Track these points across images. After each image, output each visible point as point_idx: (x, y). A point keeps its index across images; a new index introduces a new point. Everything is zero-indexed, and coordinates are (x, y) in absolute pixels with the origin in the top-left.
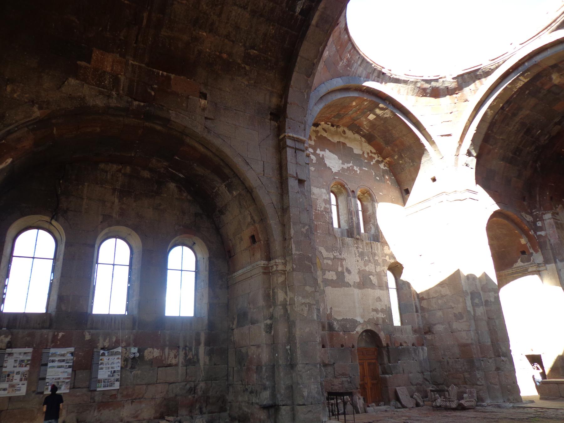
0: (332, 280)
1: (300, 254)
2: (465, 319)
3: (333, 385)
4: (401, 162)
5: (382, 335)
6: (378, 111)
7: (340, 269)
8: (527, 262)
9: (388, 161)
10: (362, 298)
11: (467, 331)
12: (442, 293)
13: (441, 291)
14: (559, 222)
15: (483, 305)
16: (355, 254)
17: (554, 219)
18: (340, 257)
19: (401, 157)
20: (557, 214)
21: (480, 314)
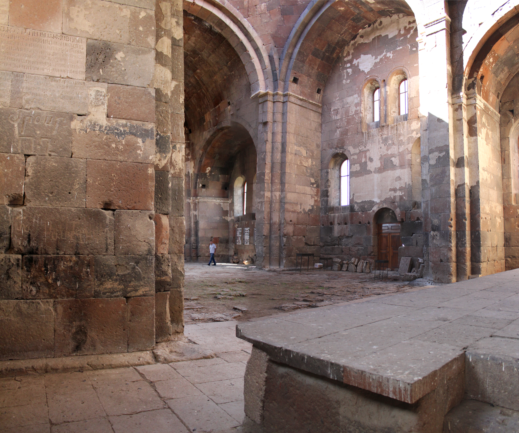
0: (356, 171)
3: (352, 251)
5: (398, 211)
7: (363, 160)
10: (381, 181)
16: (379, 142)
18: (365, 149)
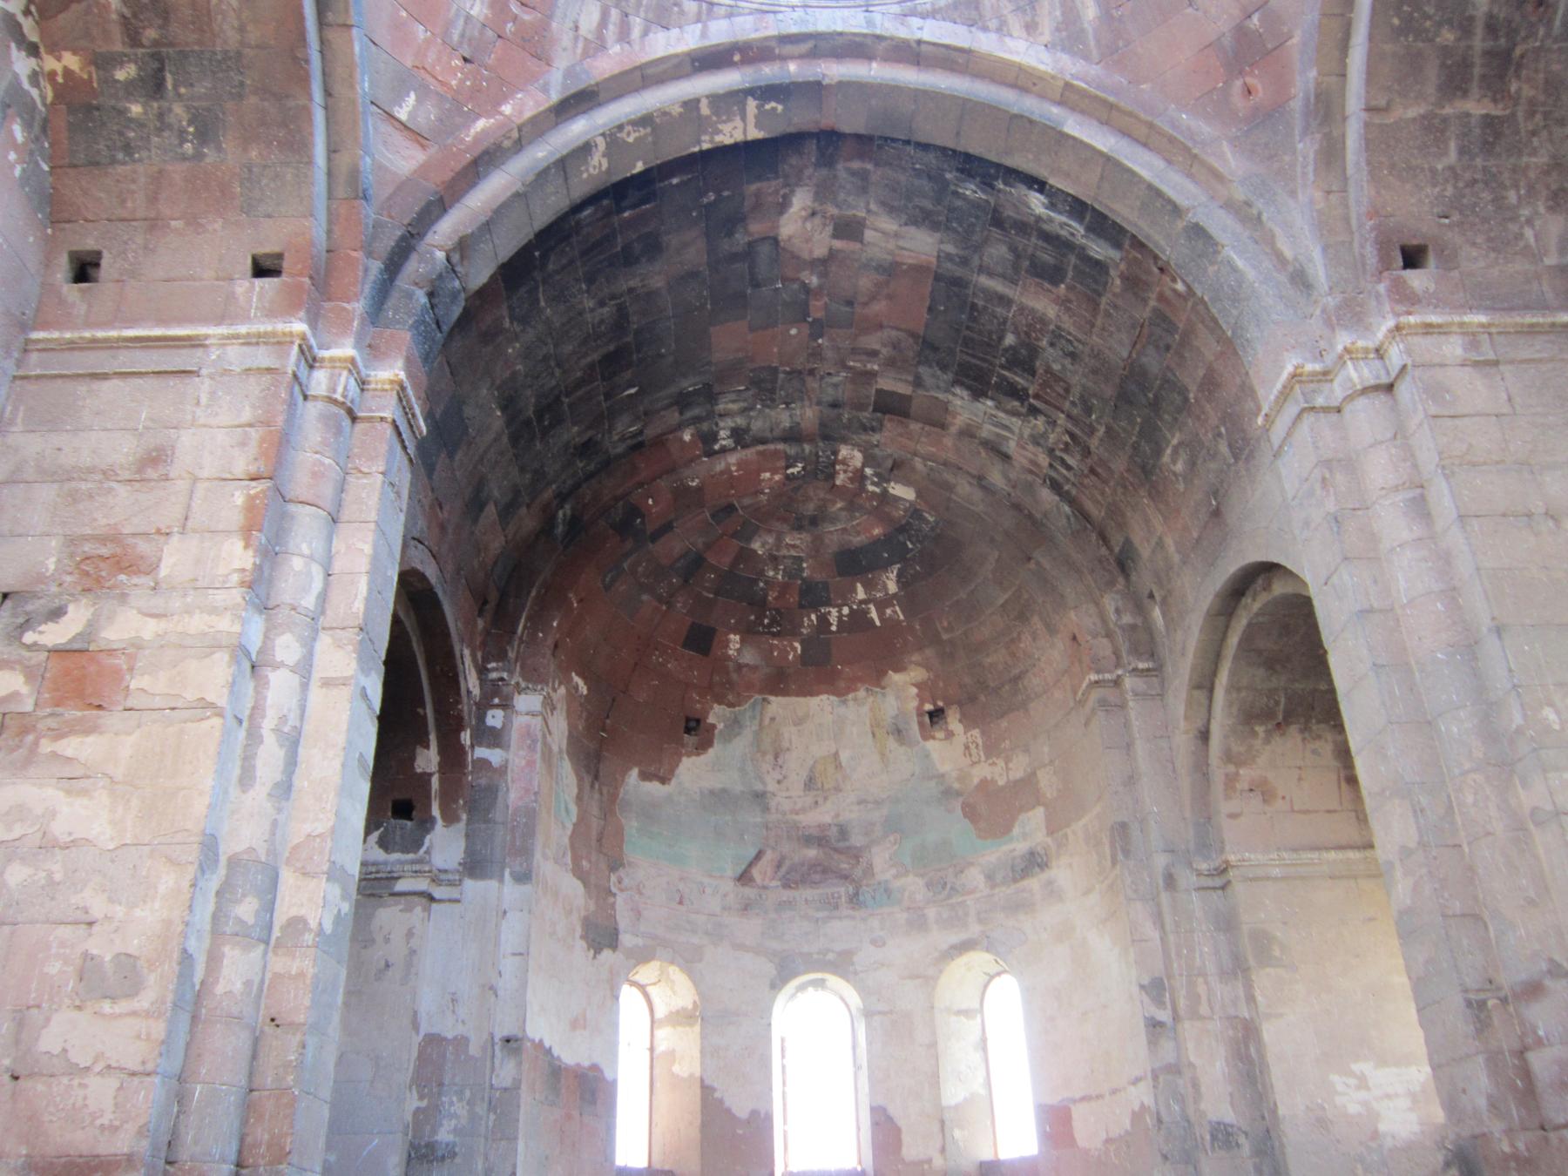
2: (144, 1002)
4: (136, 109)
8: (403, 852)
9: (67, 72)
11: (133, 1074)
12: (59, 829)
13: (52, 814)
14: (549, 739)
15: (267, 943)
19: (153, 85)
20: (553, 708)
21: (238, 986)
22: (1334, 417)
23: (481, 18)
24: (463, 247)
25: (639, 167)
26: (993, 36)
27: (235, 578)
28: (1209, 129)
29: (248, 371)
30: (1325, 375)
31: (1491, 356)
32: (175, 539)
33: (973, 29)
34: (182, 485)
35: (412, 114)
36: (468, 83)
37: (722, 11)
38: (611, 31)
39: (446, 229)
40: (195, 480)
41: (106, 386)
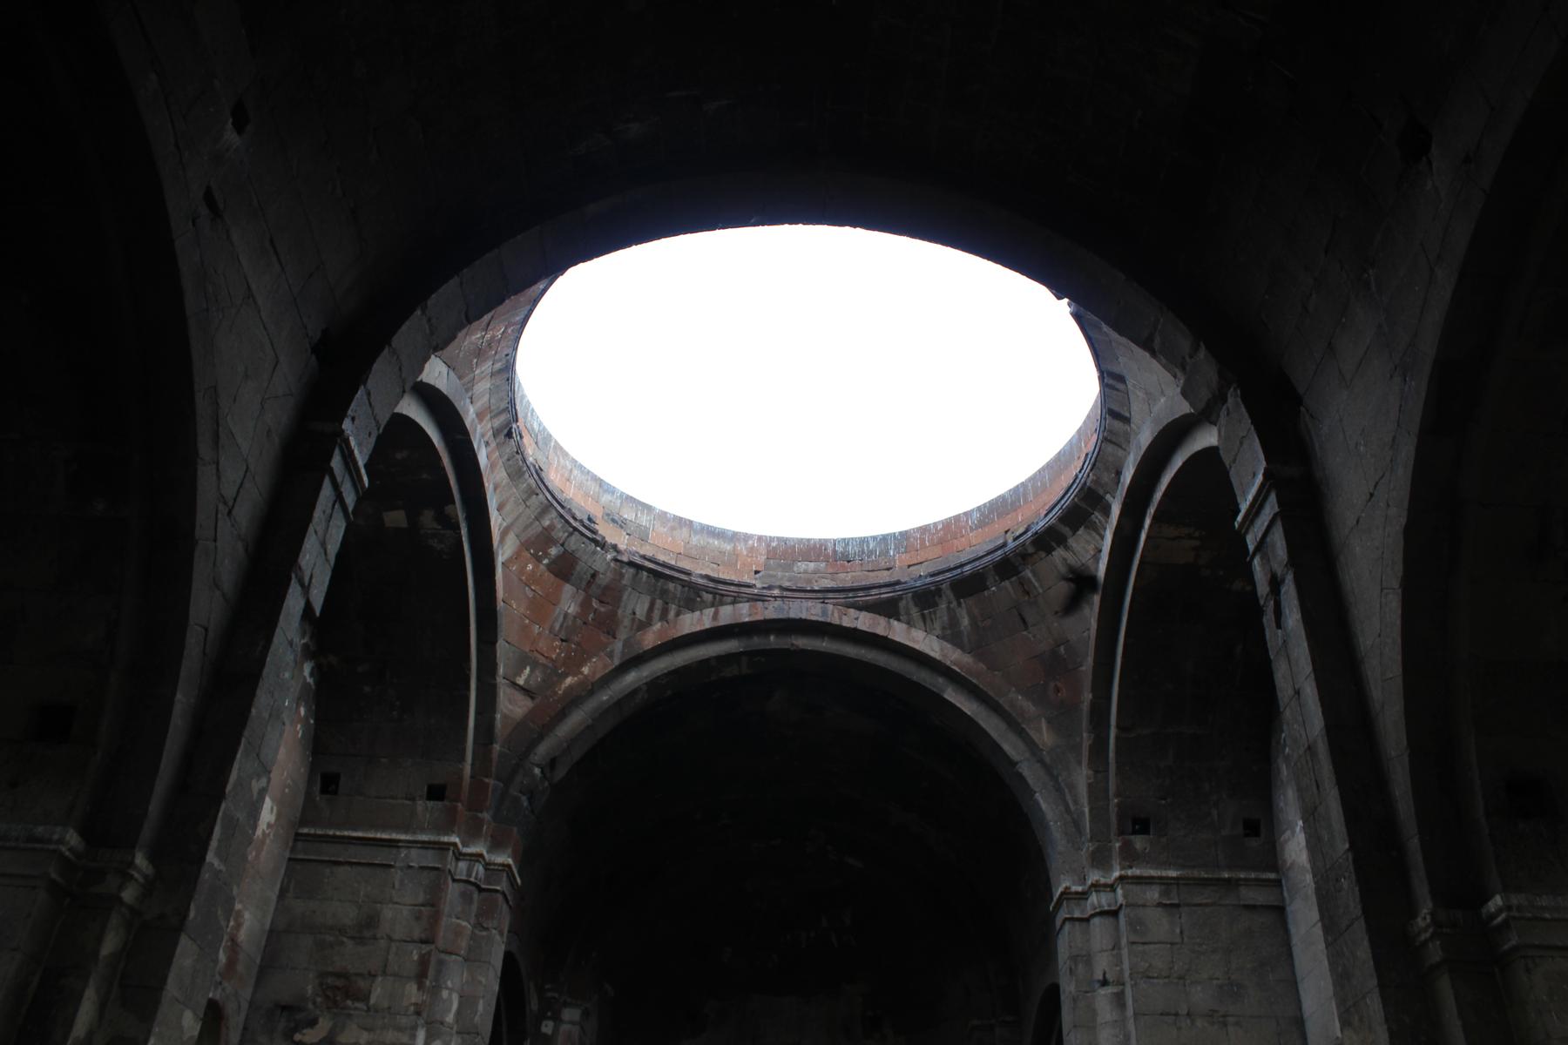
1: (221, 871)
4: (367, 689)
6: (427, 519)
17: (582, 1028)
22: (1084, 924)
23: (574, 614)
24: (553, 763)
25: (669, 692)
26: (904, 626)
27: (412, 1008)
28: (1034, 708)
29: (422, 868)
30: (1083, 896)
31: (1176, 901)
32: (380, 979)
33: (892, 620)
34: (383, 943)
35: (527, 681)
36: (563, 655)
37: (729, 599)
38: (657, 613)
39: (543, 750)
40: (390, 939)
41: (341, 870)
